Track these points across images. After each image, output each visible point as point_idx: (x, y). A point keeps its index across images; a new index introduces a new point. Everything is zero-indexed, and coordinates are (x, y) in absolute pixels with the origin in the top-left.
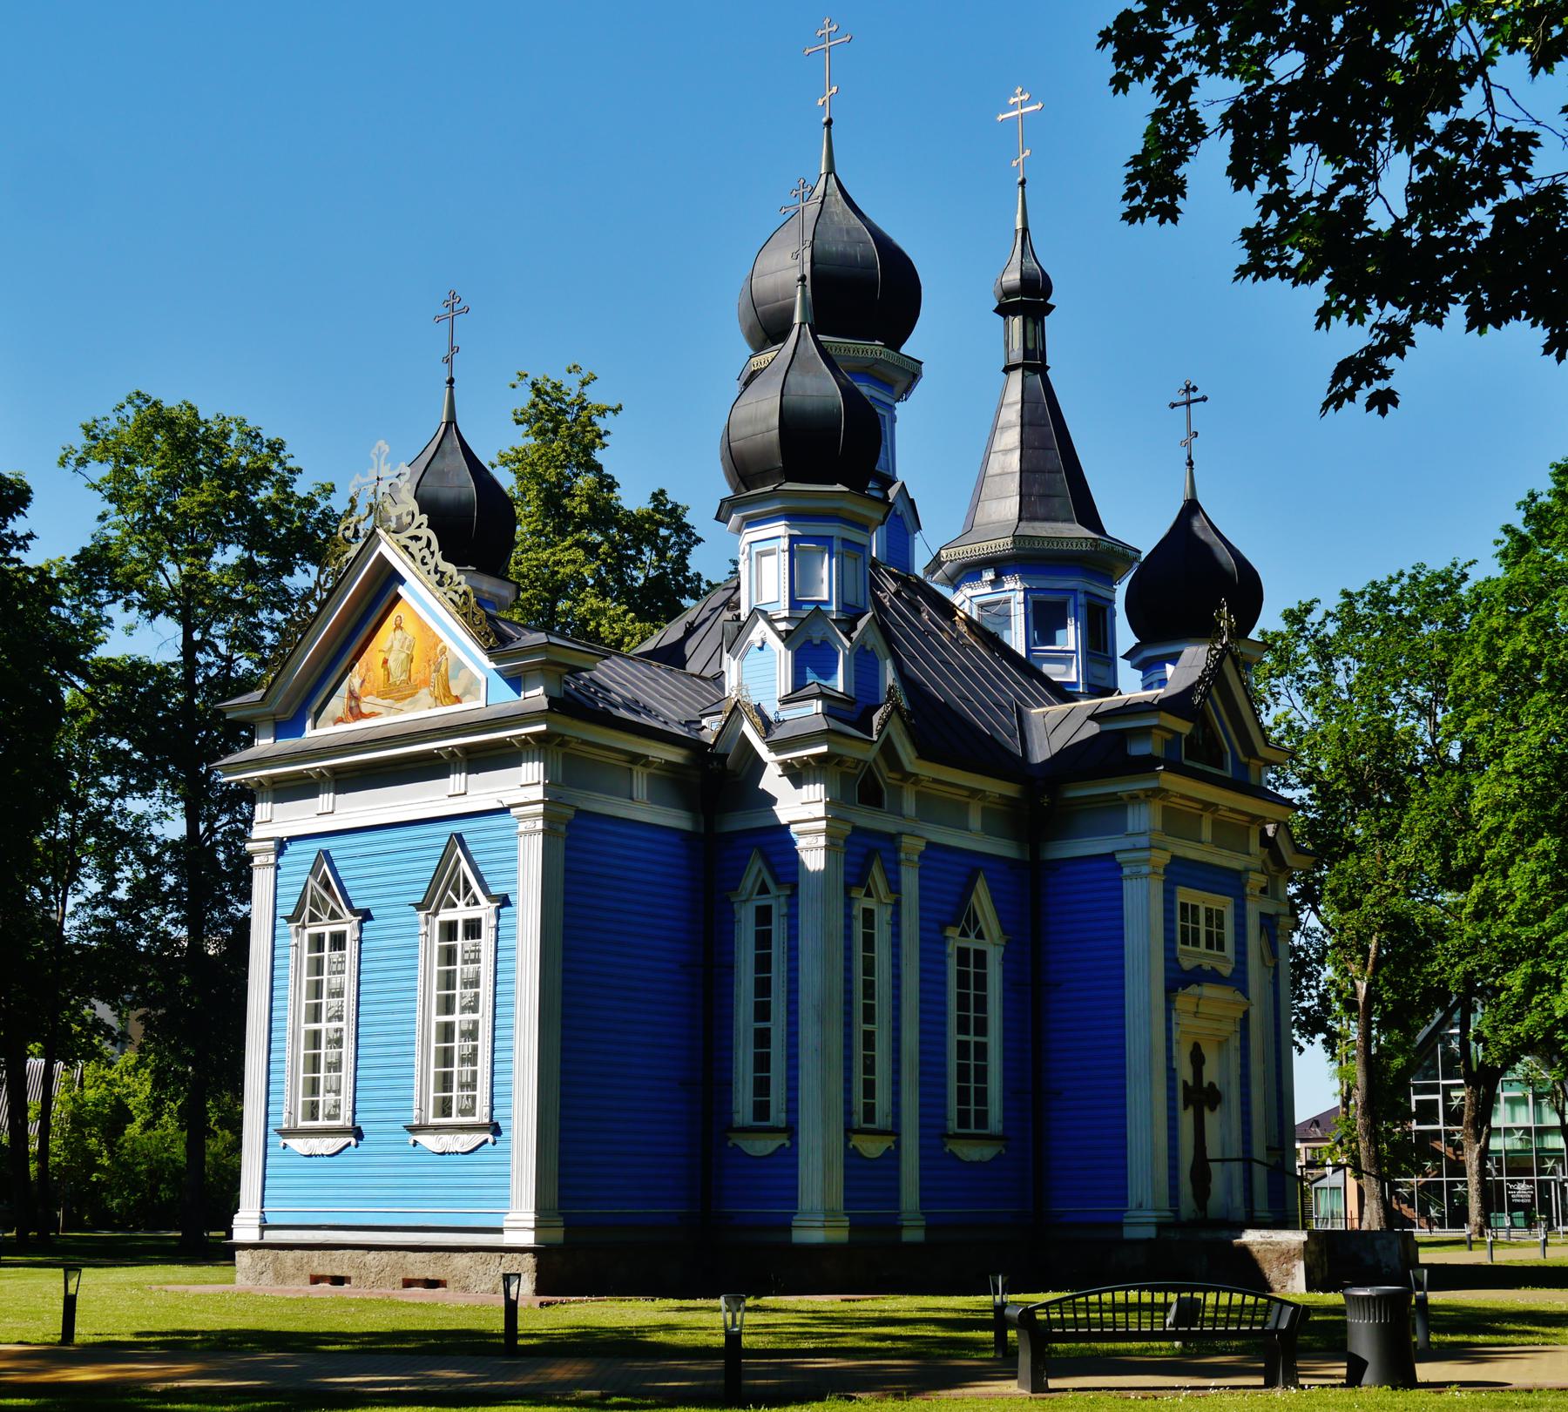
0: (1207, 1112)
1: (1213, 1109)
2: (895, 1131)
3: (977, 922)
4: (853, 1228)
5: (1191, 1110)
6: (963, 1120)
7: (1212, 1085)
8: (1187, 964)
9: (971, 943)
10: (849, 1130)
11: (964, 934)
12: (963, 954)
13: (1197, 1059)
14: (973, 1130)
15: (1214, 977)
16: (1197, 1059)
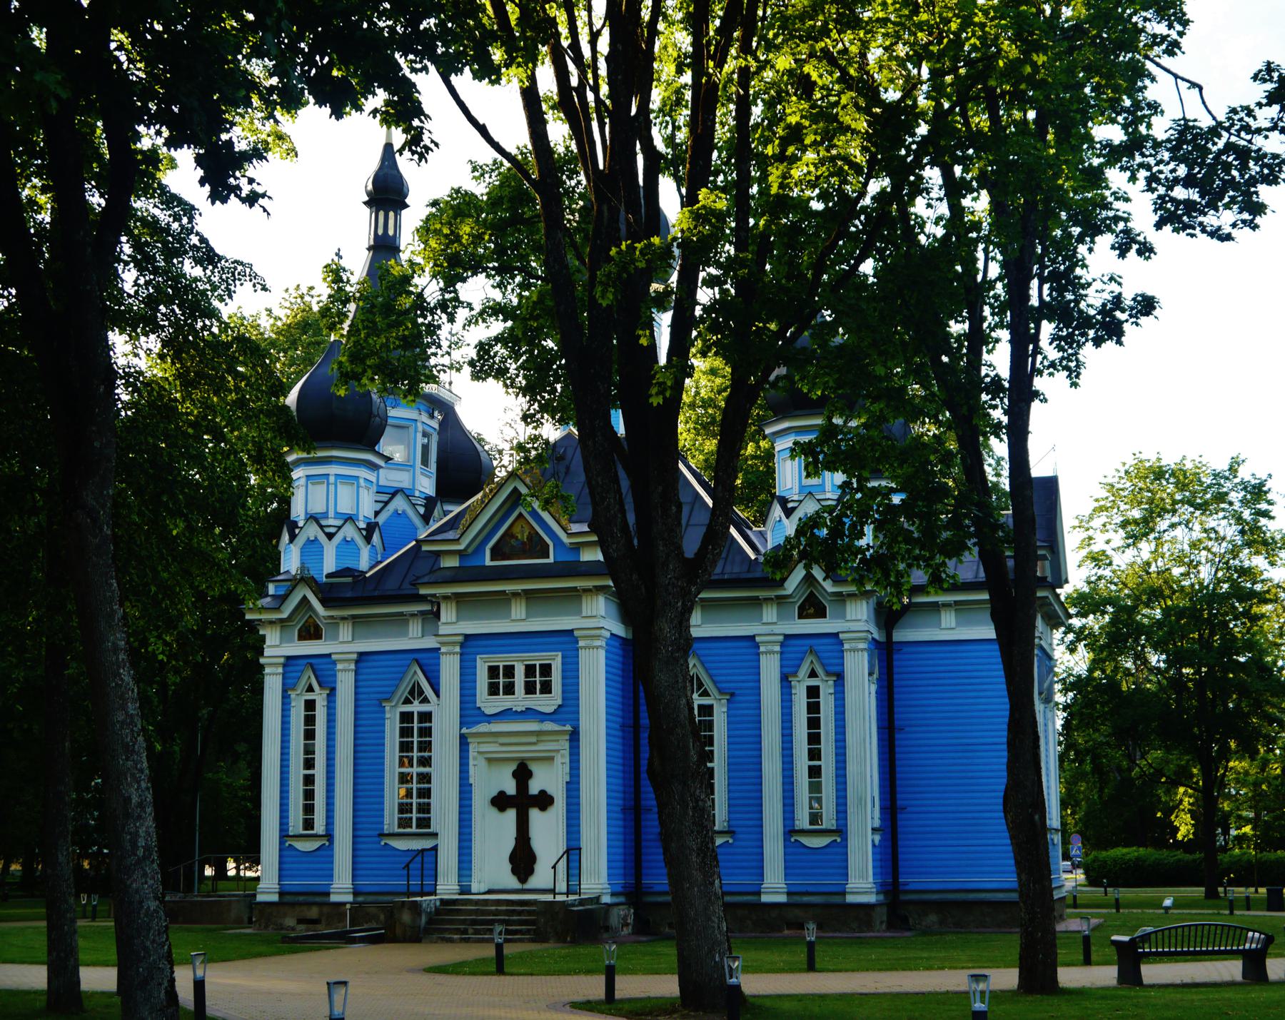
0: (534, 814)
1: (543, 808)
2: (329, 836)
3: (421, 692)
4: (281, 894)
5: (511, 814)
6: (404, 823)
7: (543, 792)
8: (488, 711)
9: (416, 707)
10: (284, 835)
11: (407, 701)
12: (406, 717)
13: (523, 774)
14: (414, 830)
15: (529, 713)
16: (523, 774)
